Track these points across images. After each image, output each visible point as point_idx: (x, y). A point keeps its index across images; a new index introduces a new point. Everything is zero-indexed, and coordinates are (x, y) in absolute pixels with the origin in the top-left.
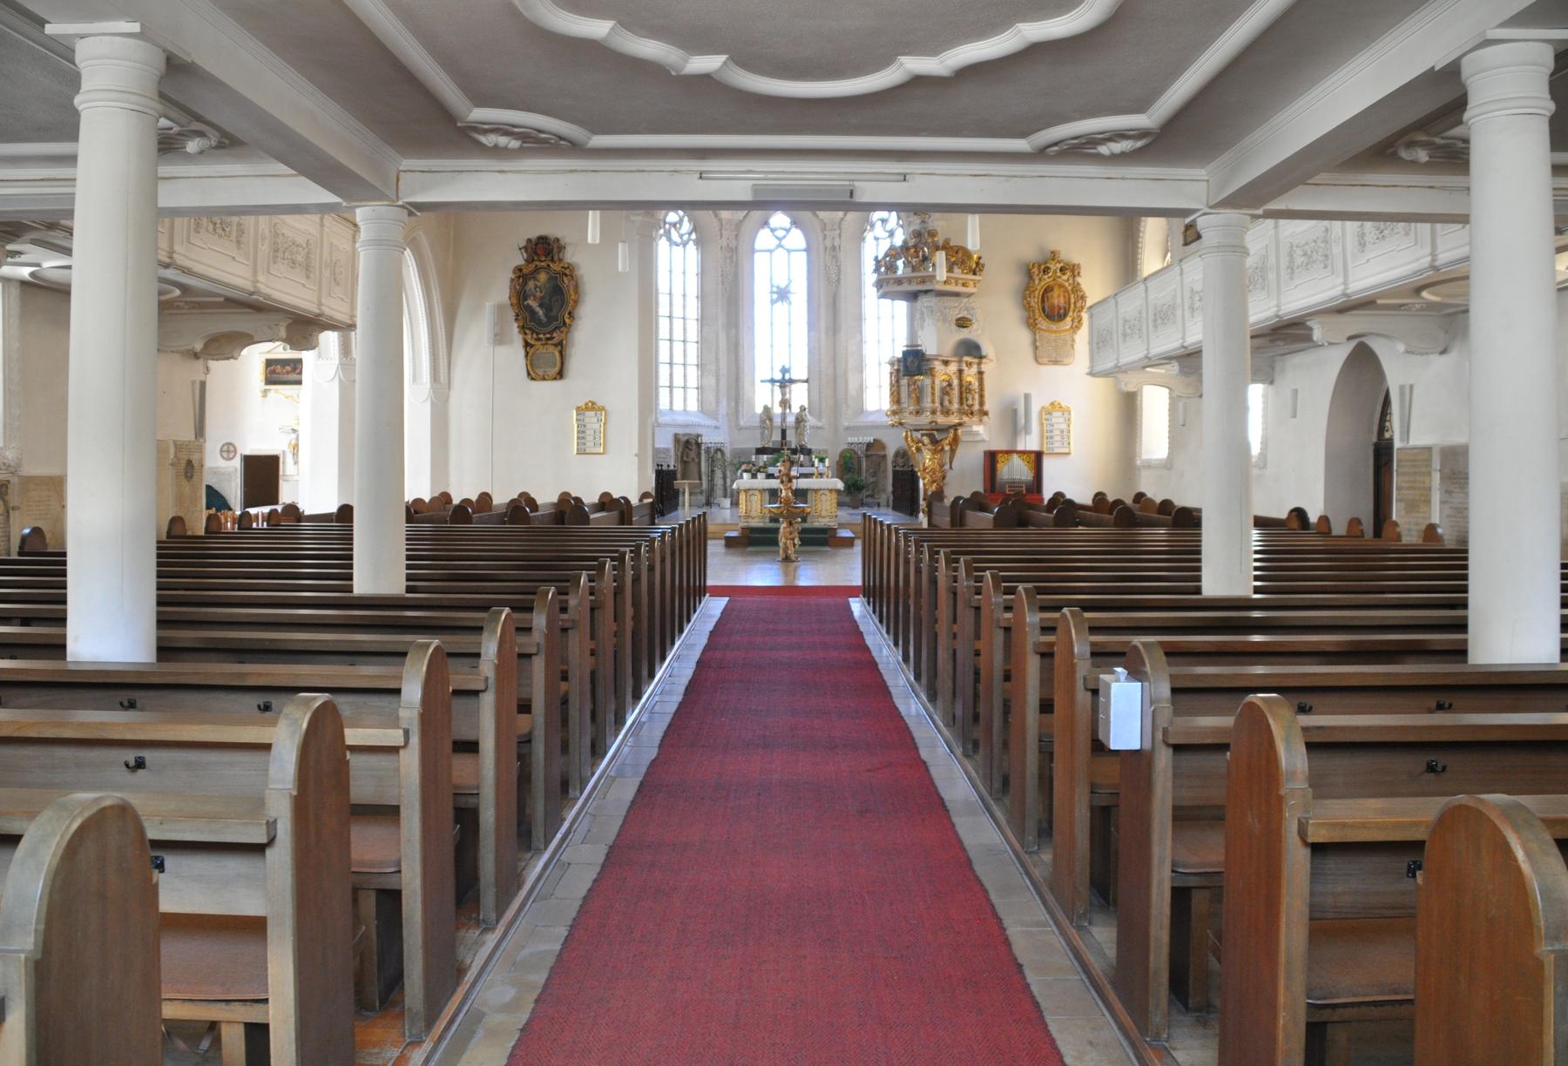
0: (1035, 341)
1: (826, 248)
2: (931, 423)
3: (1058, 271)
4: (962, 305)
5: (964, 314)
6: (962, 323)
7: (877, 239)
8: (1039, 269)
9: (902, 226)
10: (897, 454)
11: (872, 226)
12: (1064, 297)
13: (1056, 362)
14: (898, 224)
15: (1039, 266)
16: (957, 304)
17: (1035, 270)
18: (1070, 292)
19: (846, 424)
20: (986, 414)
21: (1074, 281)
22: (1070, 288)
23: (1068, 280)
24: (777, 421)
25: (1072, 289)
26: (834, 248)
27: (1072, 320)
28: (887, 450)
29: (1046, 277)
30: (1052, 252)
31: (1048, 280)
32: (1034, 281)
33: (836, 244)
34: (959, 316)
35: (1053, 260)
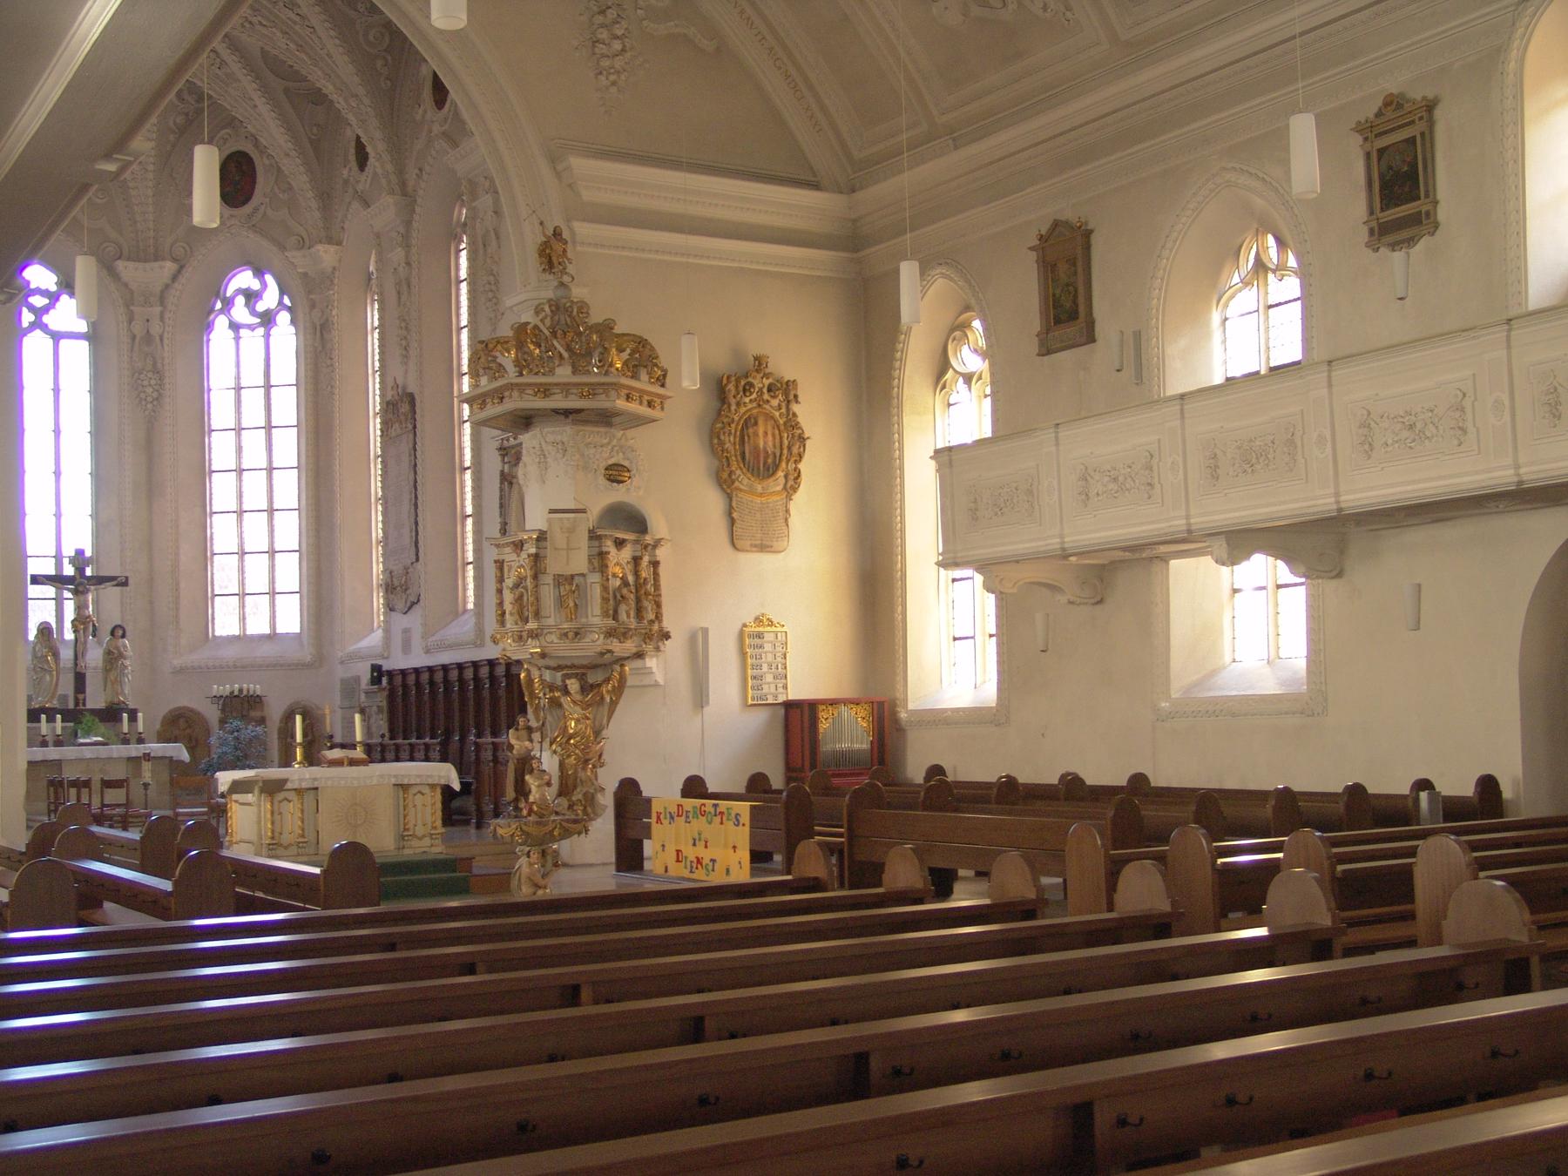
0: (729, 512)
1: (134, 338)
2: (602, 654)
3: (765, 390)
4: (615, 442)
5: (617, 458)
6: (616, 474)
7: (235, 327)
8: (737, 387)
9: (289, 309)
11: (228, 304)
12: (774, 435)
13: (763, 548)
14: (281, 302)
15: (738, 381)
16: (606, 441)
17: (731, 387)
18: (782, 428)
19: (177, 662)
20: (667, 636)
21: (788, 409)
22: (781, 422)
23: (779, 408)
25: (785, 423)
26: (148, 338)
27: (786, 477)
29: (747, 400)
30: (756, 358)
31: (750, 406)
32: (729, 406)
33: (156, 329)
34: (610, 462)
35: (757, 371)
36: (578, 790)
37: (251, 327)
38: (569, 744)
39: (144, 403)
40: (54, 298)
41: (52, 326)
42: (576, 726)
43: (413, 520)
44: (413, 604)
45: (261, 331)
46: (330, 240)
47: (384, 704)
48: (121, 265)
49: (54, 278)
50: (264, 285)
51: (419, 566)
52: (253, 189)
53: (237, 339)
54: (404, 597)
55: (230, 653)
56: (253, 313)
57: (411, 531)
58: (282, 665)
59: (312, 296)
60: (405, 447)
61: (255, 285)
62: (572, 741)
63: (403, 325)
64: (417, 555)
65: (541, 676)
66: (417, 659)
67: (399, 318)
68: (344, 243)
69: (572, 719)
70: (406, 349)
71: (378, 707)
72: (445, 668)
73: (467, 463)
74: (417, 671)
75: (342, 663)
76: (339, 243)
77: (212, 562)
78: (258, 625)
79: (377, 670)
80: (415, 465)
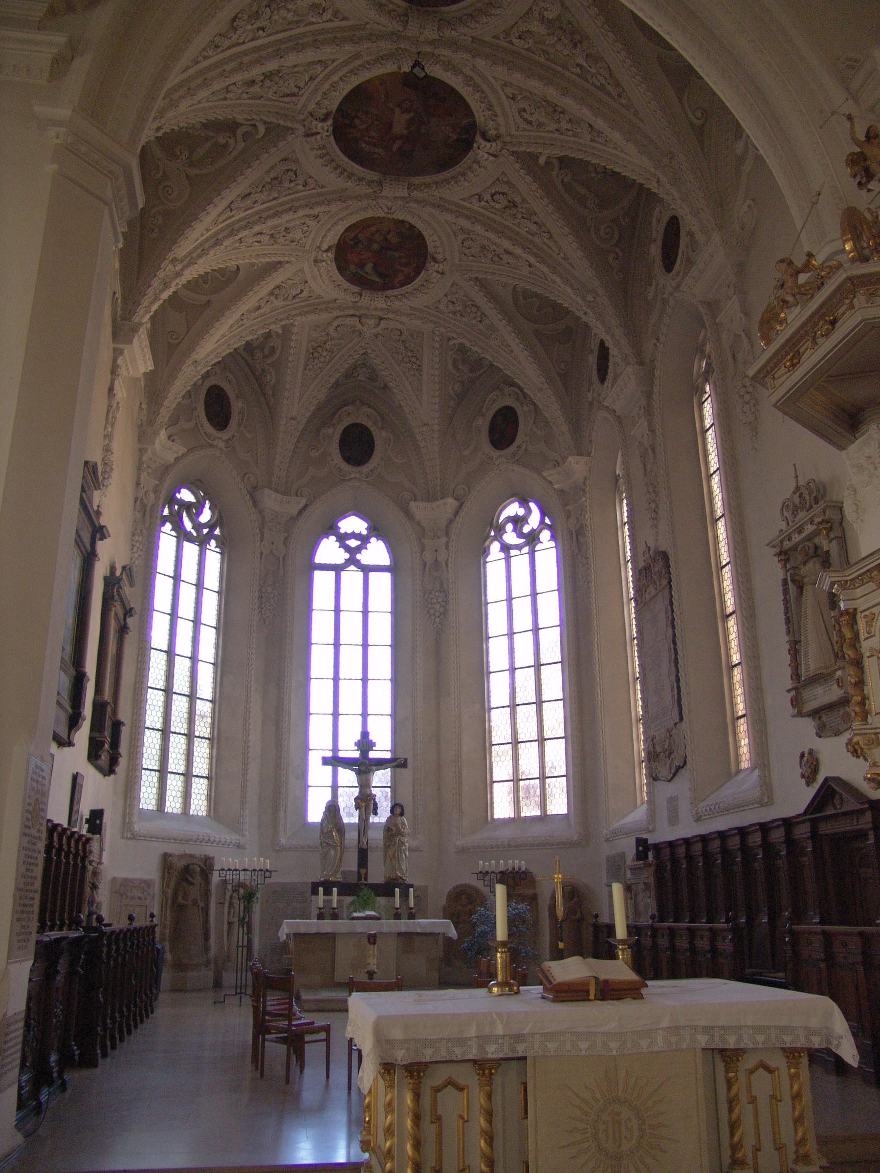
1: (425, 564)
7: (506, 548)
9: (549, 527)
11: (501, 530)
14: (542, 522)
19: (459, 843)
24: (352, 837)
33: (442, 557)
37: (519, 547)
39: (433, 617)
40: (364, 540)
41: (363, 562)
43: (673, 678)
44: (679, 768)
45: (526, 549)
46: (580, 454)
47: (651, 880)
48: (413, 504)
49: (365, 525)
50: (529, 511)
51: (684, 726)
53: (508, 559)
54: (668, 762)
55: (504, 834)
56: (520, 535)
57: (672, 690)
59: (567, 508)
60: (660, 605)
61: (521, 512)
63: (651, 489)
64: (681, 714)
66: (687, 829)
67: (646, 485)
68: (592, 454)
70: (655, 511)
71: (645, 884)
72: (722, 835)
73: (730, 609)
74: (687, 841)
75: (607, 840)
76: (589, 455)
77: (491, 752)
78: (530, 810)
79: (641, 843)
80: (673, 620)
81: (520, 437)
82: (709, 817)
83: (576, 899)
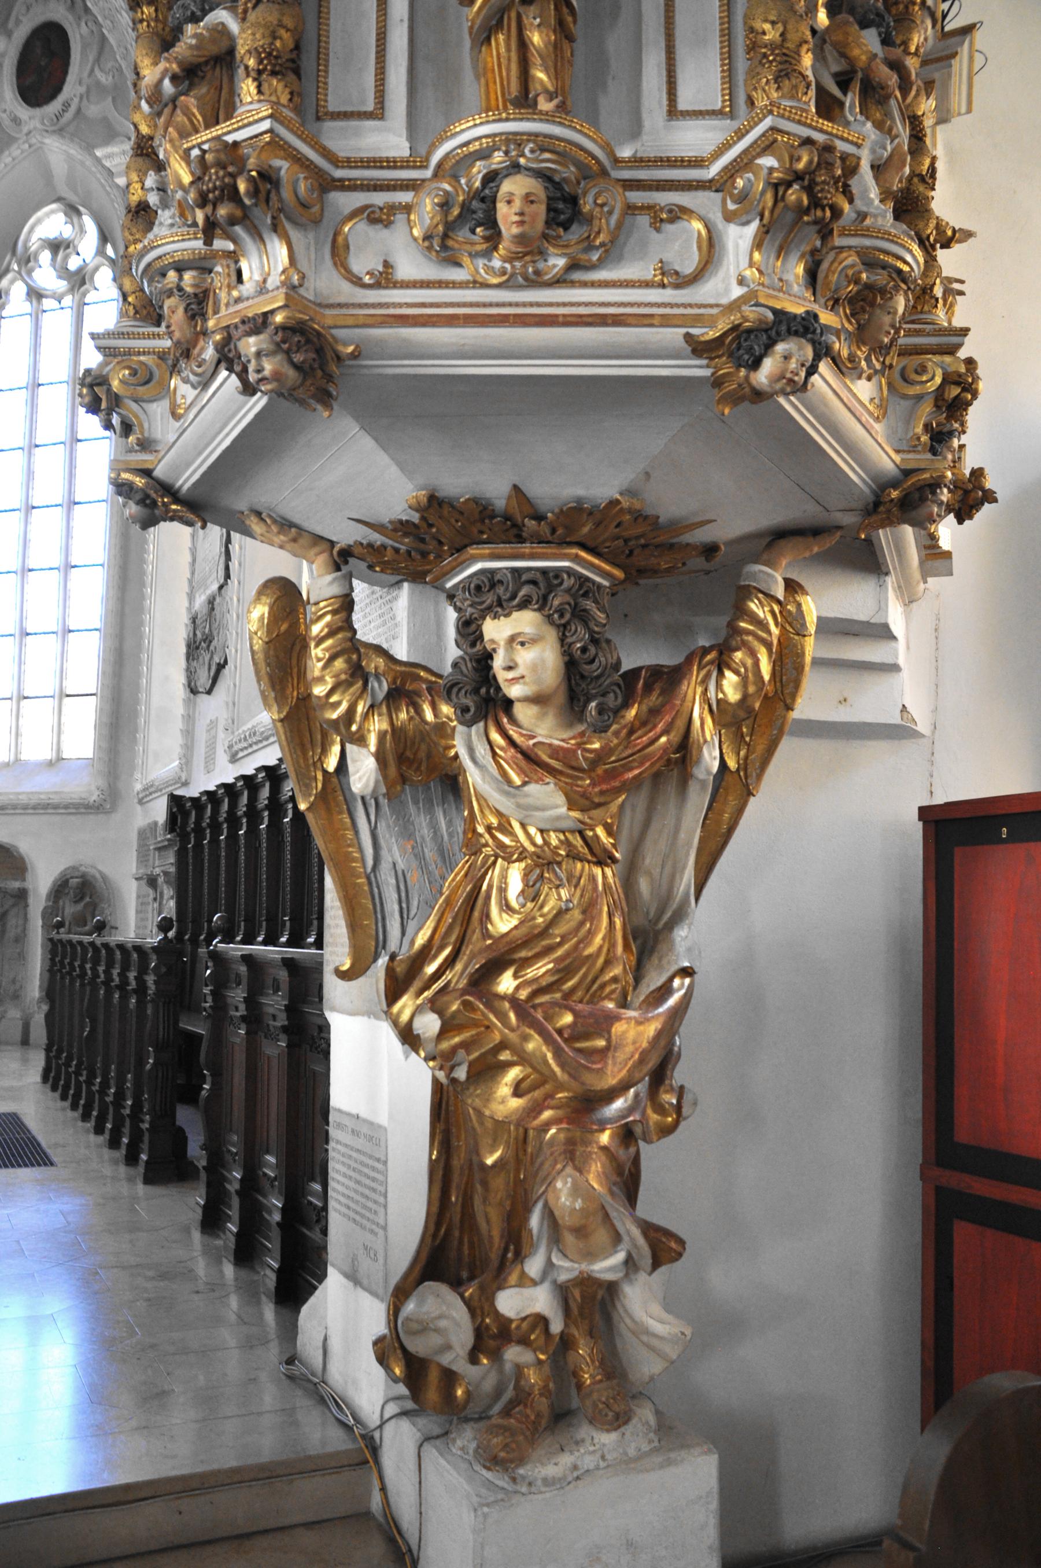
7: (35, 294)
10: (60, 889)
11: (28, 260)
14: (101, 252)
28: (29, 876)
36: (534, 1266)
38: (492, 1000)
42: (532, 892)
47: (172, 869)
50: (82, 231)
52: (65, 72)
56: (64, 272)
58: (56, 807)
61: (67, 232)
62: (506, 983)
65: (346, 604)
69: (507, 855)
71: (166, 873)
72: (248, 780)
75: (141, 802)
81: (71, 89)
82: (246, 752)
83: (88, 899)
